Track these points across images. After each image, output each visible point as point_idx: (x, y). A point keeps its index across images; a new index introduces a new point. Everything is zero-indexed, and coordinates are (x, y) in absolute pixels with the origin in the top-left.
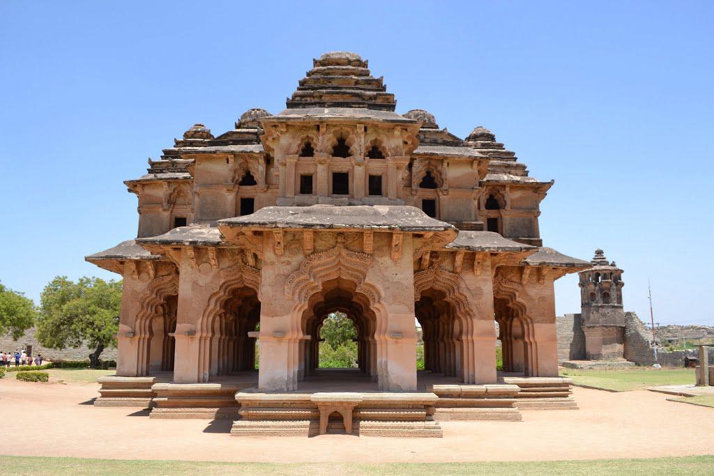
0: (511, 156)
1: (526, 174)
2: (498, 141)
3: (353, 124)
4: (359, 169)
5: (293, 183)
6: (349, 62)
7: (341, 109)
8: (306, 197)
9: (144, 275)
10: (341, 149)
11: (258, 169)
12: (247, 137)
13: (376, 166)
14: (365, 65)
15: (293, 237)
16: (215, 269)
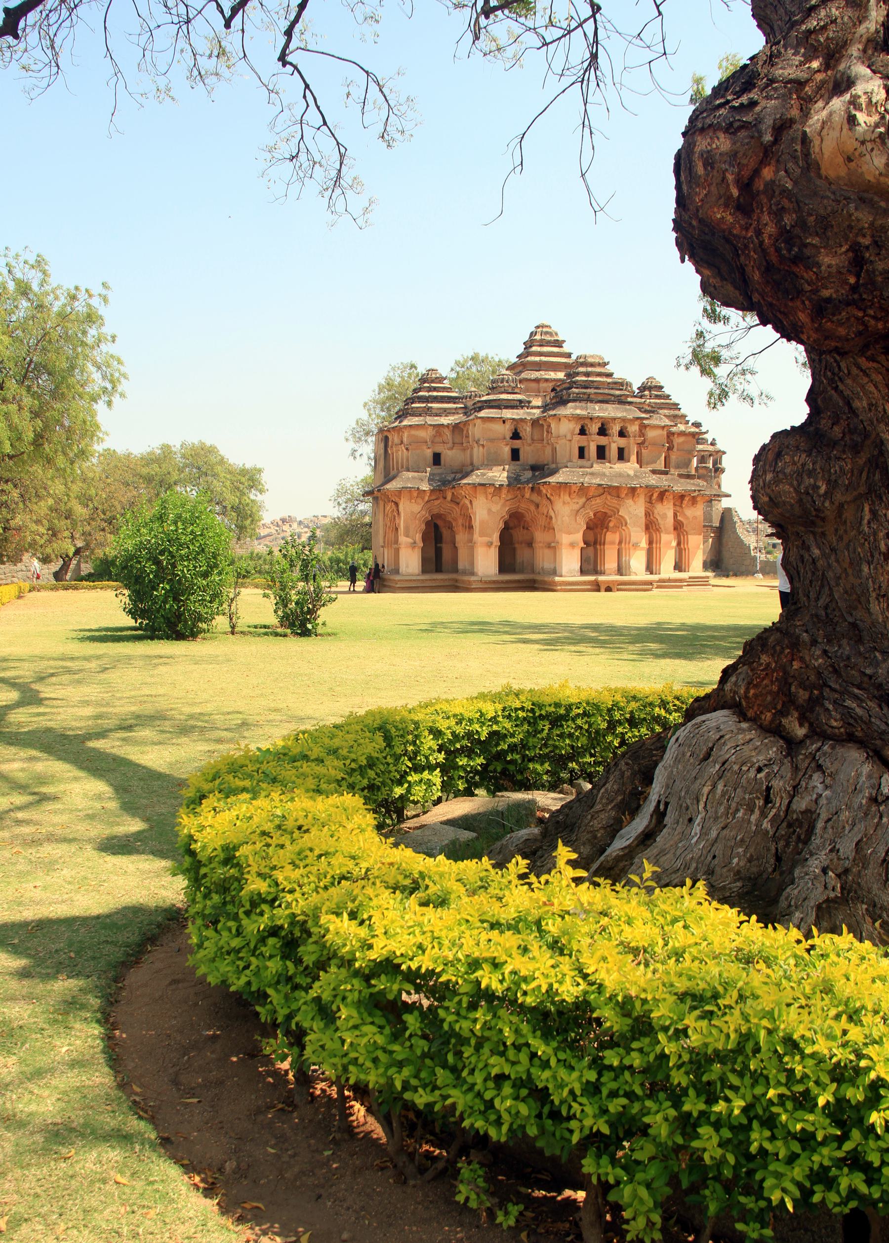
0: (676, 406)
1: (687, 422)
2: (667, 391)
3: (614, 419)
4: (614, 443)
5: (576, 452)
6: (599, 365)
7: (605, 406)
8: (581, 462)
9: (419, 500)
10: (602, 431)
11: (526, 431)
12: (512, 404)
13: (622, 442)
14: (605, 364)
15: (583, 489)
16: (502, 501)
